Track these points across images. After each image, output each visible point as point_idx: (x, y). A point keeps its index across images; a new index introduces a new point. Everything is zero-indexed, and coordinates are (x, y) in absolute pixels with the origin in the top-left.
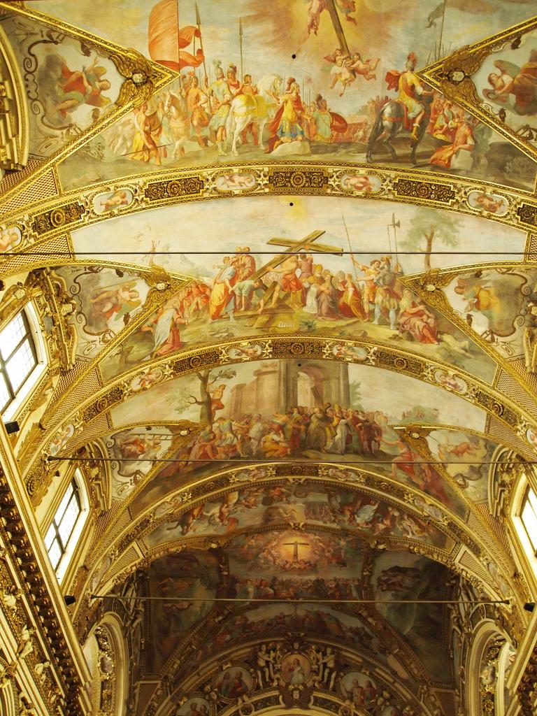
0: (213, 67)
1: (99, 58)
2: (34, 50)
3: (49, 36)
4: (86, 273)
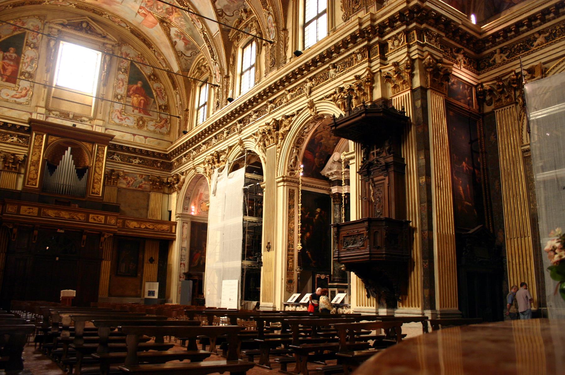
0: (138, 2)
3: (182, 55)
4: (226, 14)
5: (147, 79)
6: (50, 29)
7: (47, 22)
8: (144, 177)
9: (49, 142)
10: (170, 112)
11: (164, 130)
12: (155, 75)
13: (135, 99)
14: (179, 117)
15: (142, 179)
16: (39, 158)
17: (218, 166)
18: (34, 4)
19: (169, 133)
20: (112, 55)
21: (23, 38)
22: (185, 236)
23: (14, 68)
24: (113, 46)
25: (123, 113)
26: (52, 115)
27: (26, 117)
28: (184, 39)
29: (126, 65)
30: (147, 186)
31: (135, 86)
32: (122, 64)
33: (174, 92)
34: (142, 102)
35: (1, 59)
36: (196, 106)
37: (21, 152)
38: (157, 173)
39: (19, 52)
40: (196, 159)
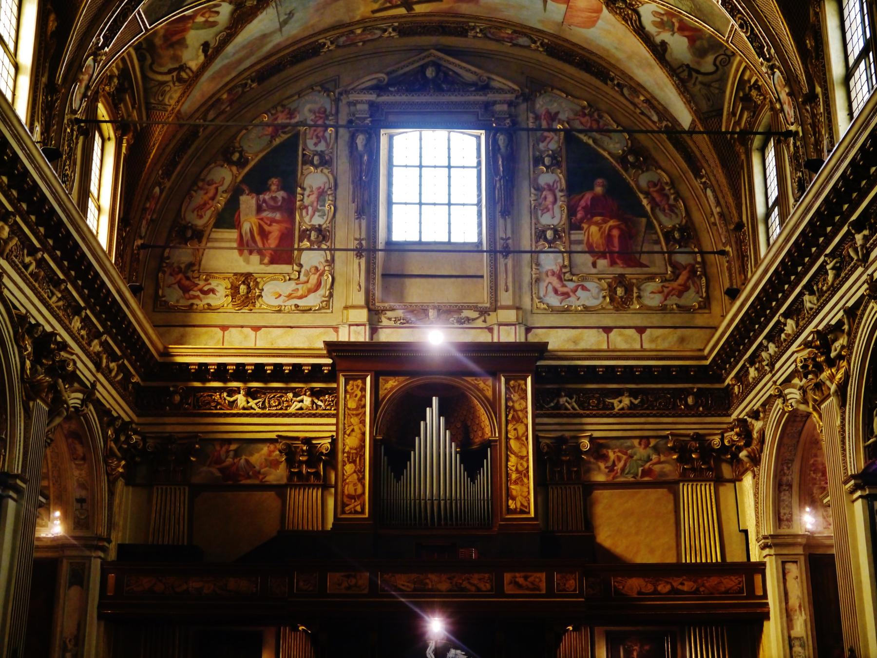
1: (655, 34)
2: (710, 68)
3: (690, 75)
5: (619, 168)
6: (352, 108)
7: (341, 94)
8: (653, 442)
9: (382, 393)
10: (699, 244)
11: (691, 298)
12: (636, 150)
13: (594, 232)
14: (723, 253)
15: (649, 451)
16: (363, 440)
17: (832, 378)
18: (303, 59)
19: (706, 304)
20: (513, 130)
21: (296, 146)
22: (794, 601)
23: (284, 225)
24: (510, 104)
25: (568, 276)
26: (385, 322)
27: (317, 339)
28: (684, 28)
29: (553, 146)
30: (667, 468)
31: (588, 196)
32: (542, 146)
33: (697, 183)
34: (615, 232)
35: (254, 212)
36: (760, 210)
37: (321, 430)
38: (688, 426)
39: (291, 185)
40: (777, 366)
